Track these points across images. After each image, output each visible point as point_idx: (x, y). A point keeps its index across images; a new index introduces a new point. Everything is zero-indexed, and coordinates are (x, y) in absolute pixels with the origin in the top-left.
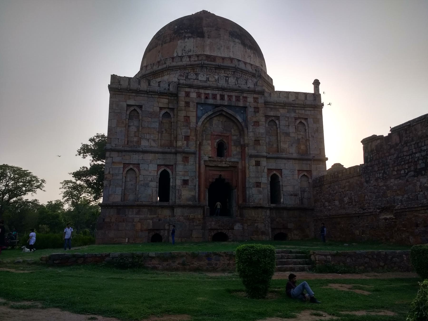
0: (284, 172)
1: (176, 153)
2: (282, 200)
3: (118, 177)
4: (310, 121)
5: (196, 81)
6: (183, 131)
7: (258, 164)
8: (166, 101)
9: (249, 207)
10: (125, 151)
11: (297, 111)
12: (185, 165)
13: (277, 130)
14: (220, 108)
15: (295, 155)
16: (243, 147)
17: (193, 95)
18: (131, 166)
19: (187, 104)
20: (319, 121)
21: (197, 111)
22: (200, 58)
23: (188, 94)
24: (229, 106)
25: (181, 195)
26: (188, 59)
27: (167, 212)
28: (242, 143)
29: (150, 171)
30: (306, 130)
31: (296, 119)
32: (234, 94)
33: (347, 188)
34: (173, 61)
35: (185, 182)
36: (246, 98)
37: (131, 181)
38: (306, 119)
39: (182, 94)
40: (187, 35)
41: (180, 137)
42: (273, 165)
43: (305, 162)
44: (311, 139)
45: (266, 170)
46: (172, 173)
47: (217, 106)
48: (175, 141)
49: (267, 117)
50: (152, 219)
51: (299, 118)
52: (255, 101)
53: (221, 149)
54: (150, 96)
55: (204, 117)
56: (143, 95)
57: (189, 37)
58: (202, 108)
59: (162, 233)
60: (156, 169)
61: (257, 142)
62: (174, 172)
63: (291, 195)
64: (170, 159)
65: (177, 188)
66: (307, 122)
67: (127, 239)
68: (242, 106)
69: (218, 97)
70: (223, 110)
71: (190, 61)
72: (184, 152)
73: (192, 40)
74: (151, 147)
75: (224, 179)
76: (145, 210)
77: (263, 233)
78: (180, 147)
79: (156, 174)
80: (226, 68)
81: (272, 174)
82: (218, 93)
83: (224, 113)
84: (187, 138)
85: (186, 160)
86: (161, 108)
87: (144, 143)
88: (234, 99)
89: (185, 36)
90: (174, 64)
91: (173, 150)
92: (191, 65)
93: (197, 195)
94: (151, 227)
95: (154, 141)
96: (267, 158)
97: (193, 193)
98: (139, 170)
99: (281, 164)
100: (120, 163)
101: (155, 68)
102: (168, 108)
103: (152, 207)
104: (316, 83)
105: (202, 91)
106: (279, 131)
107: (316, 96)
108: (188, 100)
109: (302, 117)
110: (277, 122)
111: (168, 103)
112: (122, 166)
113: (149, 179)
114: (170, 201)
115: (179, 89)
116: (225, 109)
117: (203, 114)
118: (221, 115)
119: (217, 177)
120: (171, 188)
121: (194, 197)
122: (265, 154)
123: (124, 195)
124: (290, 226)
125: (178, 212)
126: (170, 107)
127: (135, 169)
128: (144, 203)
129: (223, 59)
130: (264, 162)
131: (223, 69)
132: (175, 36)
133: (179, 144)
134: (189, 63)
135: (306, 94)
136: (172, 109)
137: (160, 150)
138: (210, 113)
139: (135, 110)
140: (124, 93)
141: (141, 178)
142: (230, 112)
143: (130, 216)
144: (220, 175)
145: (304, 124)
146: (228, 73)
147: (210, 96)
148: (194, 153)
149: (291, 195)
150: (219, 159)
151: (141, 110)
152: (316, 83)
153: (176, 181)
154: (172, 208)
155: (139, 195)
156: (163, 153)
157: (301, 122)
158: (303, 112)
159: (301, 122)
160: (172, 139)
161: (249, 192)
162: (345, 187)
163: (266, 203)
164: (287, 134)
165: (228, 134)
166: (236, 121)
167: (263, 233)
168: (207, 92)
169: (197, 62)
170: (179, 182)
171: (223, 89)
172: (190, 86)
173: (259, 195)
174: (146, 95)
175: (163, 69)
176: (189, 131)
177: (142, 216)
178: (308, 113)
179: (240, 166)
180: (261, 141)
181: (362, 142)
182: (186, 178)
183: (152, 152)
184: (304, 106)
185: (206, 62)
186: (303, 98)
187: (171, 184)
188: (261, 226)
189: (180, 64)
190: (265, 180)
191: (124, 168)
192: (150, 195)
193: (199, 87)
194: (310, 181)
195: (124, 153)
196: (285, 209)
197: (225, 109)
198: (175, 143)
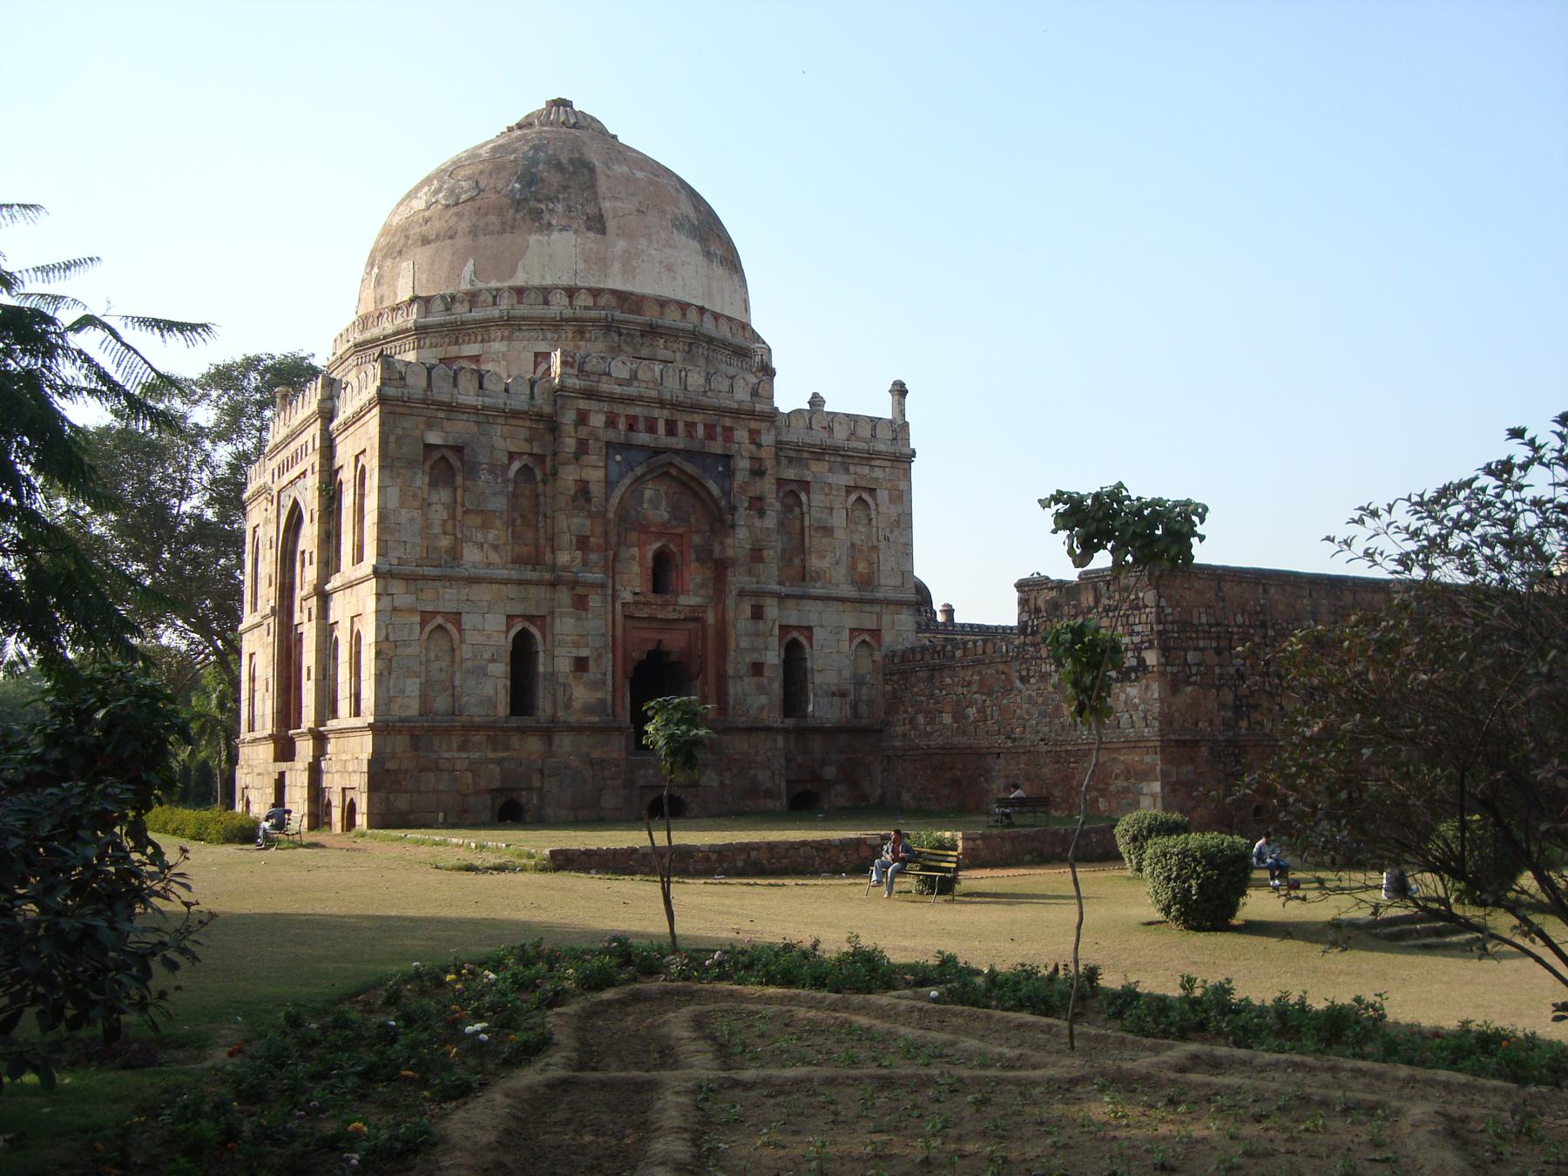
0: (818, 634)
1: (553, 585)
2: (810, 708)
3: (410, 651)
4: (883, 495)
5: (604, 379)
6: (570, 524)
7: (758, 613)
8: (524, 433)
9: (738, 729)
10: (425, 578)
11: (852, 469)
12: (578, 619)
13: (802, 520)
14: (664, 458)
15: (847, 590)
16: (720, 568)
17: (597, 420)
18: (439, 620)
19: (582, 446)
20: (902, 497)
21: (606, 467)
22: (602, 301)
23: (582, 418)
24: (689, 454)
25: (570, 699)
26: (566, 301)
27: (534, 745)
28: (717, 554)
29: (488, 632)
30: (870, 520)
31: (849, 490)
32: (697, 418)
33: (975, 688)
34: (520, 302)
35: (581, 664)
36: (730, 429)
37: (437, 658)
38: (872, 491)
39: (569, 417)
40: (554, 222)
41: (566, 538)
42: (793, 617)
43: (867, 608)
44: (882, 545)
45: (776, 631)
46: (544, 637)
47: (657, 452)
48: (548, 550)
49: (780, 482)
50: (499, 762)
51: (856, 487)
52: (753, 442)
53: (661, 574)
54: (481, 419)
55: (627, 481)
56: (464, 417)
57: (563, 229)
58: (618, 458)
59: (523, 797)
60: (504, 628)
61: (756, 555)
62: (549, 636)
63: (833, 694)
64: (537, 599)
65: (562, 680)
66: (875, 499)
67: (441, 815)
68: (720, 452)
69: (661, 428)
70: (671, 464)
71: (571, 304)
72: (574, 584)
73: (569, 236)
74: (489, 565)
75: (668, 653)
76: (478, 738)
77: (769, 794)
78: (566, 568)
79: (503, 642)
80: (671, 334)
81: (789, 637)
82: (661, 416)
83: (674, 472)
84: (583, 543)
85: (580, 603)
86: (512, 456)
87: (471, 555)
88: (700, 431)
89: (550, 225)
90: (522, 310)
91: (547, 576)
92: (575, 320)
93: (609, 698)
94: (497, 784)
95: (495, 548)
96: (782, 598)
97: (599, 695)
98: (460, 630)
99: (811, 614)
100: (412, 610)
101: (461, 311)
102: (530, 454)
103: (494, 732)
104: (900, 390)
105: (619, 409)
106: (807, 524)
107: (899, 428)
108: (583, 432)
109: (864, 484)
110: (804, 497)
111: (529, 440)
112: (417, 619)
113: (487, 656)
114: (540, 713)
115: (559, 402)
116: (677, 460)
117: (622, 476)
118: (666, 474)
119: (651, 646)
120: (541, 679)
121: (603, 701)
122: (775, 587)
123: (425, 698)
124: (830, 772)
125: (565, 742)
126: (535, 451)
127: (449, 626)
128: (476, 719)
129: (663, 303)
130: (772, 610)
131: (661, 335)
132: (519, 216)
133: (564, 558)
134: (568, 313)
135: (874, 422)
136: (540, 459)
137: (514, 575)
138: (639, 471)
139: (443, 458)
140: (415, 411)
141: (466, 651)
142: (690, 469)
143: (446, 755)
144: (660, 642)
145: (866, 503)
146: (675, 346)
147: (641, 425)
148: (603, 586)
149: (833, 694)
150: (658, 599)
151: (462, 460)
152: (900, 390)
153: (555, 661)
154: (548, 731)
155: (465, 700)
156: (520, 582)
157: (860, 499)
158: (866, 470)
159: (860, 499)
160: (542, 542)
161: (734, 689)
162: (970, 684)
163: (774, 718)
164: (827, 531)
165: (680, 530)
166: (703, 494)
167: (769, 794)
168: (636, 411)
169: (593, 314)
170: (564, 665)
171: (675, 406)
172: (590, 394)
173: (758, 699)
174: (473, 418)
175: (488, 320)
176: (588, 522)
177: (475, 755)
178: (878, 473)
179: (711, 619)
180: (765, 553)
181: (1021, 586)
182: (584, 653)
183: (492, 581)
184: (869, 457)
185: (618, 315)
186: (865, 432)
187: (541, 669)
188: (763, 776)
189: (539, 310)
190: (773, 657)
191: (423, 623)
192: (490, 699)
193: (611, 398)
194: (878, 656)
195: (420, 584)
196: (820, 730)
197: (677, 460)
198: (548, 556)
